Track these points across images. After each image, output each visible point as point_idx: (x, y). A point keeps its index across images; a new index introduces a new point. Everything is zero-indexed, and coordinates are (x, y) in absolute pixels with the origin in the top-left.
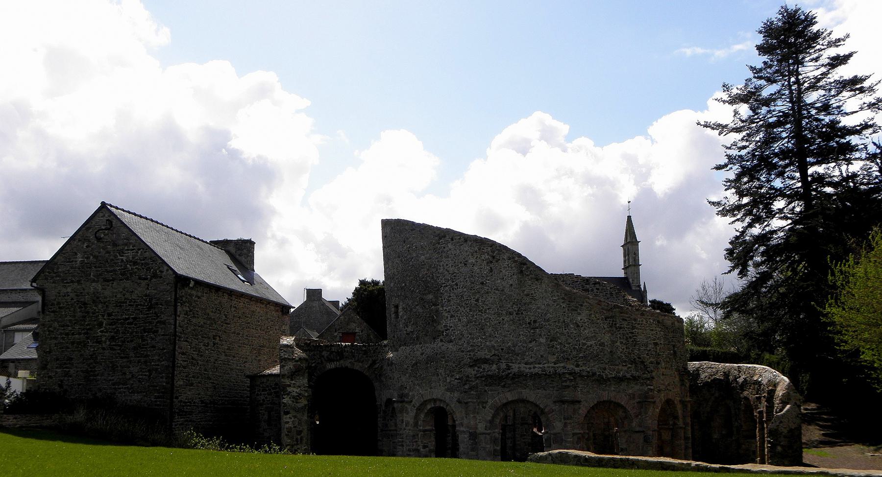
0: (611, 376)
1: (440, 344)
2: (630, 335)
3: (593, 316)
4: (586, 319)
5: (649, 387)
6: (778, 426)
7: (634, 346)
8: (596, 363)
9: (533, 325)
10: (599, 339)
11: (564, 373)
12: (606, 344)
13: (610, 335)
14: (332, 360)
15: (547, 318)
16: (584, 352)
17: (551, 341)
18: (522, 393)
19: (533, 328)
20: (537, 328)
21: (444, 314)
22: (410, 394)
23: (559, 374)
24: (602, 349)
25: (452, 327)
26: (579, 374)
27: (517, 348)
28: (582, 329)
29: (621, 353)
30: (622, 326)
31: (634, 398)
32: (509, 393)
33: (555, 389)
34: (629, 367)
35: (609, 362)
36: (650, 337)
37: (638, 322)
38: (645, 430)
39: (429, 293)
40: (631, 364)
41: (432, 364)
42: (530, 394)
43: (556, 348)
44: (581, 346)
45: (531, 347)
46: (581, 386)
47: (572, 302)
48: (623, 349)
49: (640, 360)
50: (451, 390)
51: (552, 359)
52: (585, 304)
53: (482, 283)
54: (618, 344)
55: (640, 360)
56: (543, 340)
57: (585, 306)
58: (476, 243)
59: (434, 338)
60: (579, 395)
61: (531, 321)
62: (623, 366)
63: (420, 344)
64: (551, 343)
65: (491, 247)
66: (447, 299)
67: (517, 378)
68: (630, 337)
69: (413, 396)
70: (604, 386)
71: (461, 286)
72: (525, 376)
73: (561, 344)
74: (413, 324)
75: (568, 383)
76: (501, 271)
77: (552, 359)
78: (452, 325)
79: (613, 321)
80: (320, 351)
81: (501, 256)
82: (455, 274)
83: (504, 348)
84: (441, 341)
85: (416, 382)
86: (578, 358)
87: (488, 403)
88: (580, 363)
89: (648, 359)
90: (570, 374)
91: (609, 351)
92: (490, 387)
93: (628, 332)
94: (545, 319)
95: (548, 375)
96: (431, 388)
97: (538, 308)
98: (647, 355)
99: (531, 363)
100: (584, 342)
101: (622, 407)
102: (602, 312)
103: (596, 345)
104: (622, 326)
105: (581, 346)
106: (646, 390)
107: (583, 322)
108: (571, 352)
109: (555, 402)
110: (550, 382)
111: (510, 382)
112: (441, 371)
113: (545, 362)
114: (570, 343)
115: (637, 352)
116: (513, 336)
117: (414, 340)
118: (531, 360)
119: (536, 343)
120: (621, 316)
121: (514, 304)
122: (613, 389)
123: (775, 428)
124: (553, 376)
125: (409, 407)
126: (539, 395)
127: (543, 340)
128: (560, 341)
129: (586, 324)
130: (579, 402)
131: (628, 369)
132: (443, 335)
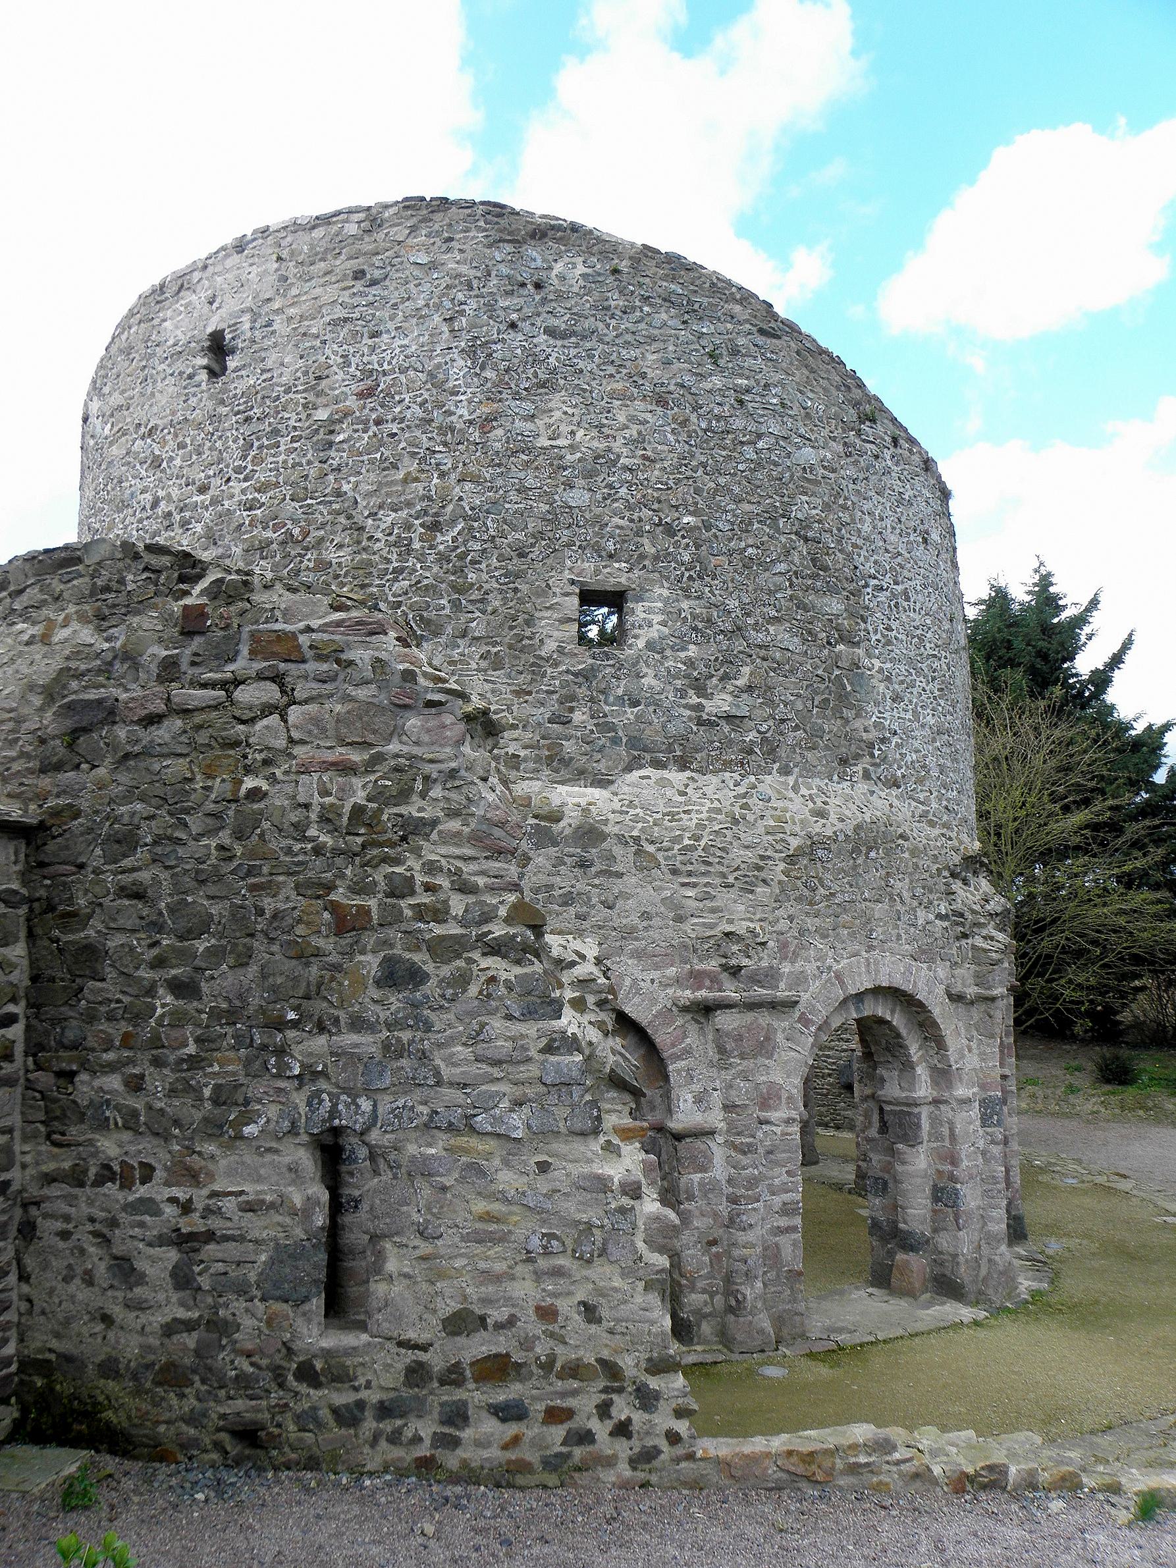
1: (863, 787)
21: (874, 682)
22: (786, 968)
25: (895, 733)
39: (832, 590)
41: (873, 854)
50: (924, 955)
59: (844, 762)
63: (785, 771)
66: (883, 636)
69: (800, 980)
71: (918, 606)
74: (749, 689)
78: (895, 726)
82: (899, 559)
84: (867, 776)
85: (811, 924)
96: (870, 948)
112: (901, 886)
117: (751, 752)
125: (781, 1025)
132: (872, 755)
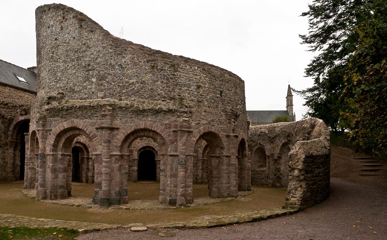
0: (148, 108)
2: (172, 76)
3: (136, 59)
4: (130, 61)
5: (184, 118)
6: (298, 151)
7: (176, 86)
8: (137, 98)
9: (88, 68)
10: (141, 78)
11: (104, 105)
12: (147, 82)
13: (151, 75)
14: (22, 115)
15: (97, 61)
16: (127, 89)
17: (101, 80)
18: (74, 122)
19: (87, 71)
20: (91, 70)
23: (101, 105)
24: (143, 86)
26: (118, 106)
27: (76, 88)
28: (126, 69)
29: (161, 90)
30: (163, 68)
31: (170, 128)
32: (65, 122)
33: (99, 118)
34: (168, 102)
35: (149, 97)
36: (193, 80)
37: (181, 67)
38: (179, 155)
40: (171, 100)
42: (80, 123)
43: (104, 86)
44: (124, 84)
45: (85, 86)
46: (120, 116)
47: (118, 48)
48: (164, 88)
49: (179, 97)
51: (100, 94)
52: (129, 49)
53: (56, 39)
54: (159, 83)
55: (179, 97)
56: (94, 80)
57: (129, 50)
58: (55, 9)
60: (117, 123)
61: (86, 65)
62: (163, 101)
64: (101, 82)
65: (63, 10)
67: (70, 110)
68: (171, 78)
70: (142, 116)
72: (75, 108)
73: (108, 82)
75: (106, 113)
76: (68, 28)
77: (100, 94)
79: (155, 64)
80: (16, 109)
81: (68, 16)
83: (68, 88)
86: (121, 94)
87: (52, 131)
88: (122, 98)
89: (188, 97)
90: (110, 105)
91: (150, 88)
92: (54, 118)
93: (169, 73)
94: (96, 63)
95: (92, 107)
97: (92, 54)
98: (189, 94)
99: (85, 99)
100: (127, 80)
101: (160, 135)
102: (144, 56)
103: (138, 83)
104: (163, 68)
105: (124, 84)
106: (181, 121)
107: (126, 64)
108: (116, 89)
109: (97, 129)
110: (94, 113)
111: (64, 113)
113: (95, 97)
114: (115, 82)
115: (178, 91)
116: (74, 78)
118: (86, 96)
119: (89, 82)
120: (163, 60)
121: (75, 52)
122: (150, 119)
123: (295, 154)
124: (96, 107)
126: (86, 123)
127: (94, 80)
128: (107, 80)
129: (130, 66)
130: (118, 129)
131: (166, 103)
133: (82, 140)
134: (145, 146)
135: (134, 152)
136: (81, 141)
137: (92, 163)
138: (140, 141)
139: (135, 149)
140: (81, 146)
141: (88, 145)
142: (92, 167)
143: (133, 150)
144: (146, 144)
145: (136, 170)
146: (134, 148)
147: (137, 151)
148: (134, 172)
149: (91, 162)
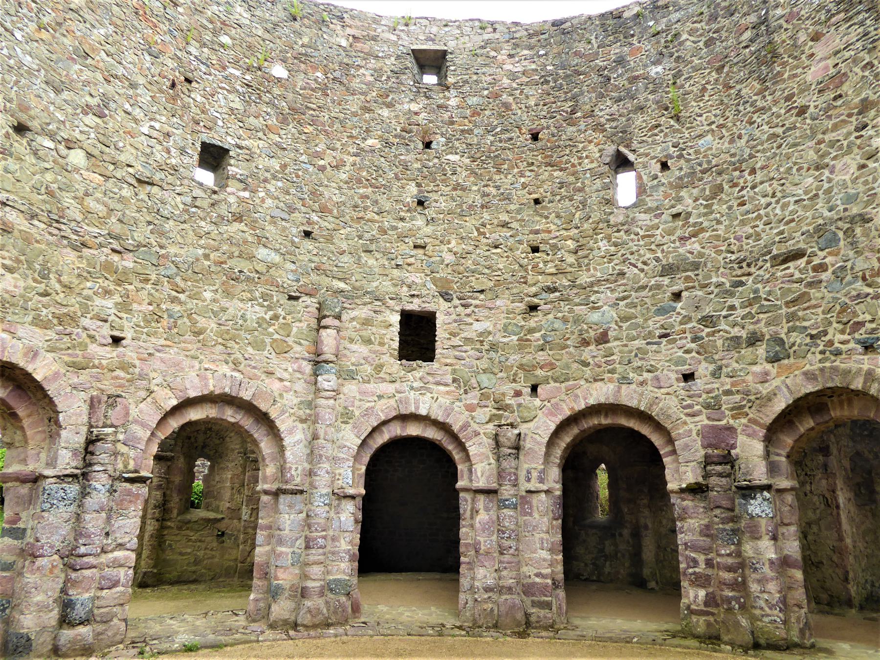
133: (427, 406)
134: (810, 388)
135: (741, 439)
136: (423, 412)
137: (495, 518)
138: (768, 366)
139: (744, 421)
140: (431, 434)
141: (466, 426)
142: (494, 538)
143: (730, 429)
144: (810, 376)
145: (771, 562)
146: (734, 417)
147: (762, 433)
148: (754, 576)
149: (487, 509)
